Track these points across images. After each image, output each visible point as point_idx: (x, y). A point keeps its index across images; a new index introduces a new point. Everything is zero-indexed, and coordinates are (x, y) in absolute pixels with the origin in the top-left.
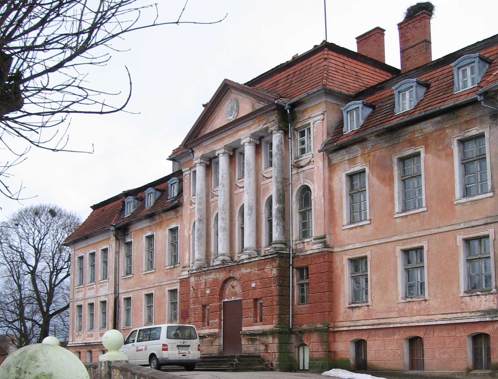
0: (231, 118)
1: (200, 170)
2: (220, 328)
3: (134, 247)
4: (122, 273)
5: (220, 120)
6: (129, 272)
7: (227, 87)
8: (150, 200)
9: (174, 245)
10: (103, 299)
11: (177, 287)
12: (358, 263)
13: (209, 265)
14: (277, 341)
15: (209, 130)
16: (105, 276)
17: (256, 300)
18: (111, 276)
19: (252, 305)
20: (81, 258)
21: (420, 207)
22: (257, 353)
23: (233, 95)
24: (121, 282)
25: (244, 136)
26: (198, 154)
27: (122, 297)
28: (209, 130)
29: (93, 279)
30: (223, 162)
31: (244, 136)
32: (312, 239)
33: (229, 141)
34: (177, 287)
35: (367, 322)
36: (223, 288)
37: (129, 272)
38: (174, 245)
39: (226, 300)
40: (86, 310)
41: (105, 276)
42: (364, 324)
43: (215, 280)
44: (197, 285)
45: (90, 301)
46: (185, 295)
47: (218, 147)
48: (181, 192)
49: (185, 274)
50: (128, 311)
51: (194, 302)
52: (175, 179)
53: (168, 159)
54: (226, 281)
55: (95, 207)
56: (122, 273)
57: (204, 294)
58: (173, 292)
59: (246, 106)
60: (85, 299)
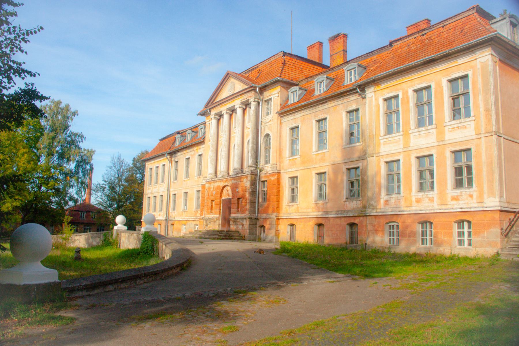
0: (231, 93)
1: (214, 122)
2: (220, 214)
3: (179, 163)
4: (172, 179)
5: (225, 93)
6: (176, 178)
7: (227, 76)
8: (189, 138)
9: (200, 163)
10: (161, 194)
11: (200, 189)
12: (293, 179)
13: (242, 171)
14: (248, 223)
15: (218, 99)
16: (163, 181)
17: (239, 199)
18: (166, 181)
19: (236, 202)
20: (151, 169)
21: (399, 132)
22: (238, 230)
23: (232, 80)
24: (172, 184)
25: (237, 103)
26: (213, 112)
27: (172, 193)
28: (218, 99)
29: (156, 183)
30: (226, 117)
31: (237, 103)
32: (269, 165)
33: (229, 105)
34: (200, 189)
35: (296, 214)
36: (222, 190)
37: (176, 178)
38: (200, 163)
39: (224, 198)
40: (152, 199)
41: (163, 181)
42: (295, 215)
43: (219, 186)
44: (209, 188)
45: (155, 195)
46: (203, 193)
47: (224, 109)
48: (204, 133)
49: (204, 182)
50: (175, 202)
51: (207, 199)
52: (202, 126)
53: (198, 115)
54: (224, 187)
55: (162, 140)
56: (172, 179)
57: (212, 195)
58: (198, 191)
59: (239, 86)
60: (152, 193)
